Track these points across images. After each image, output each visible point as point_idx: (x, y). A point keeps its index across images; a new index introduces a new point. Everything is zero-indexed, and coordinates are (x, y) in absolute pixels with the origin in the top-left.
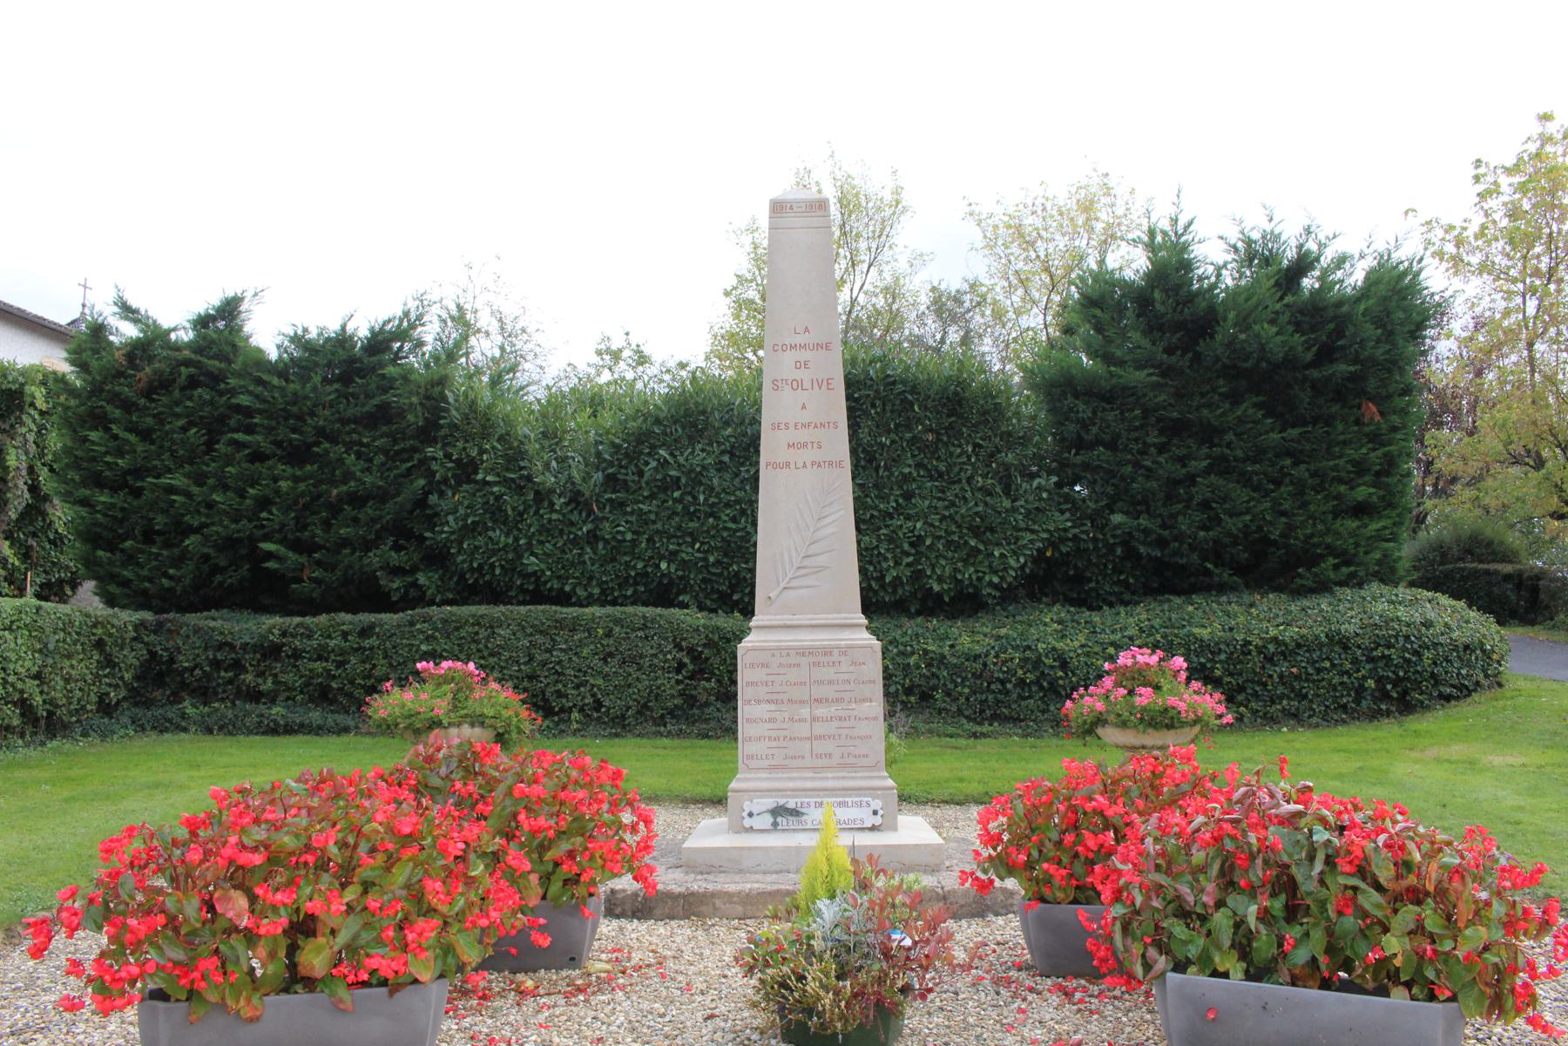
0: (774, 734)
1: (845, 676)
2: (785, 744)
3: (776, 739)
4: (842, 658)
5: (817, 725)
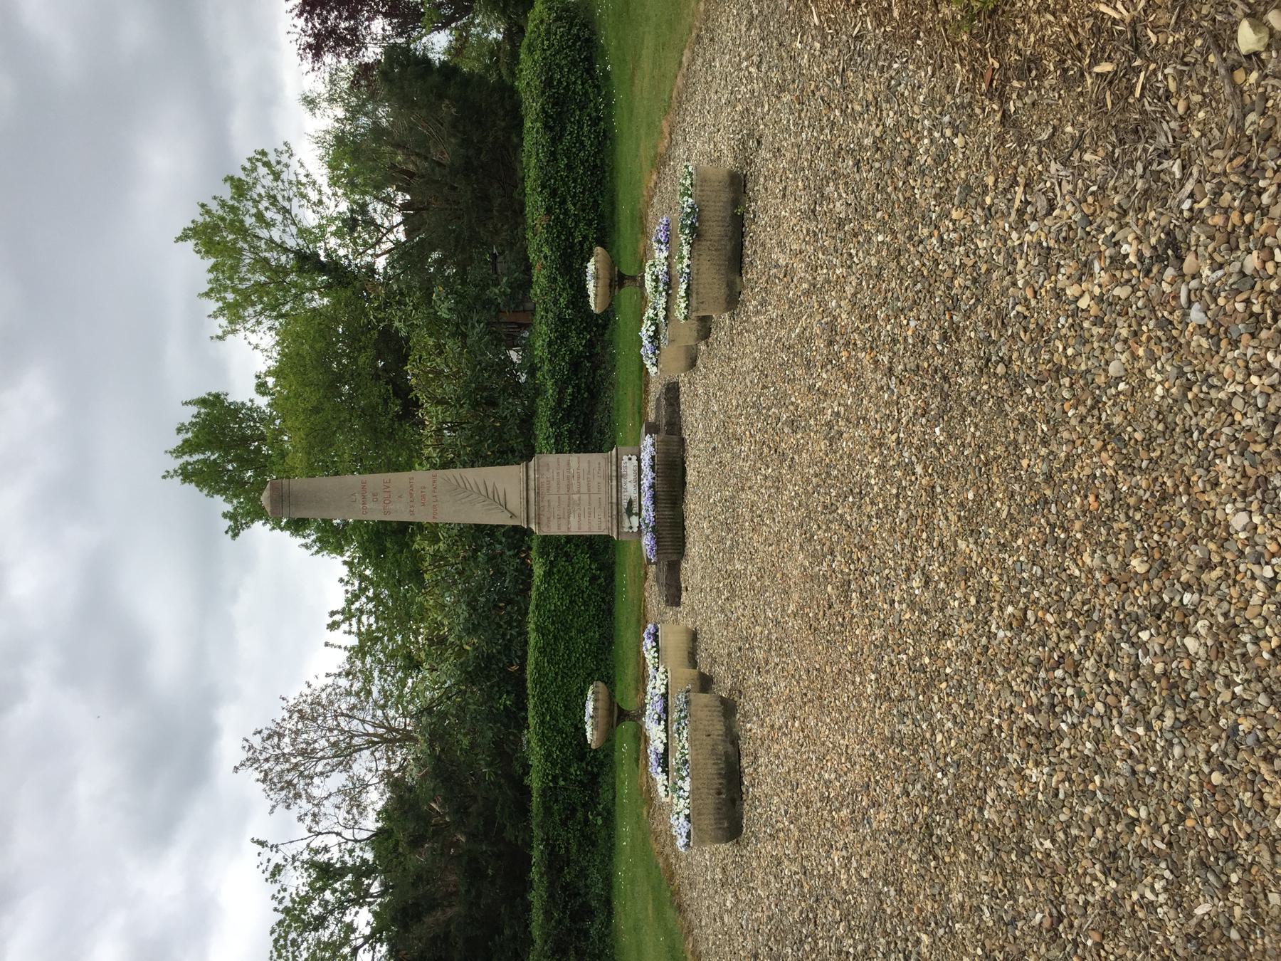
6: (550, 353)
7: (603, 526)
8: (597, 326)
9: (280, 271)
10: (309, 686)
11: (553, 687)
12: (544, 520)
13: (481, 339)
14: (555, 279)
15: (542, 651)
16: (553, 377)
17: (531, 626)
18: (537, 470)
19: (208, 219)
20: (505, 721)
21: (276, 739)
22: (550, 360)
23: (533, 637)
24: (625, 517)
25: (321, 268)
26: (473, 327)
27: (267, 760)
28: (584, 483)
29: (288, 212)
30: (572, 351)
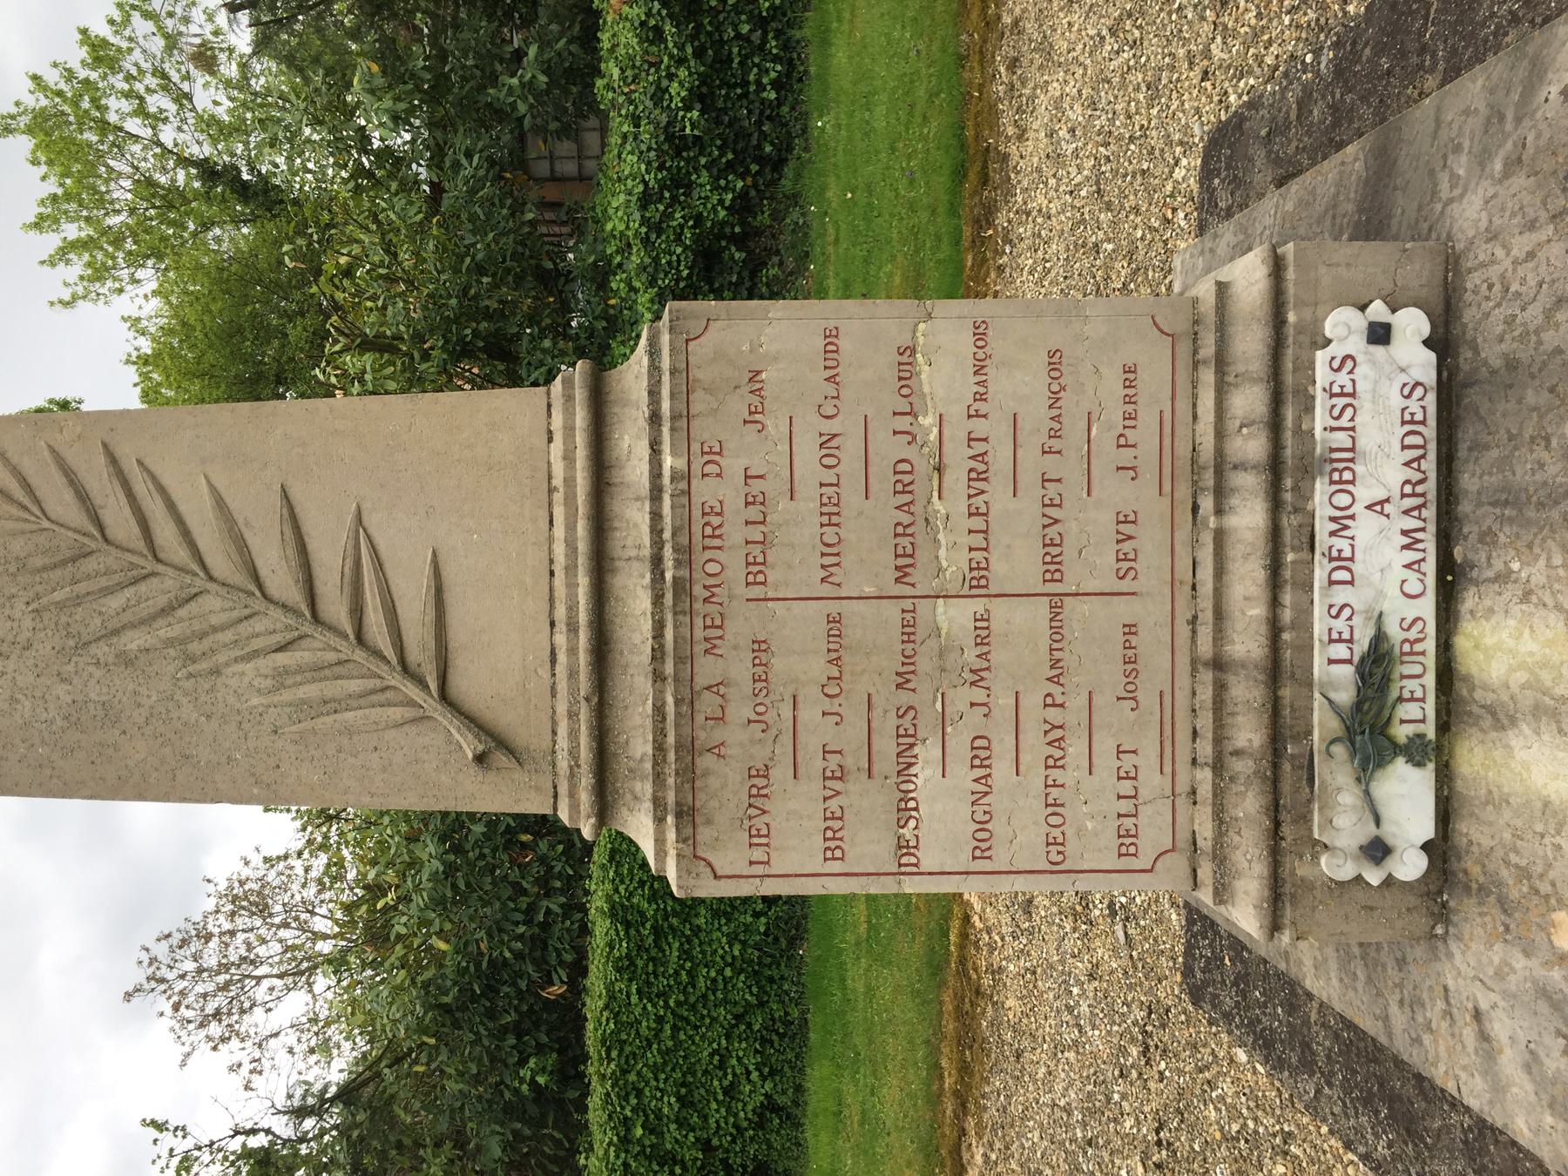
0: (1035, 747)
1: (807, 451)
2: (1077, 702)
3: (1055, 736)
4: (734, 465)
5: (1002, 572)
6: (644, 221)
7: (1154, 831)
8: (761, 160)
9: (172, 200)
10: (247, 863)
11: (653, 1056)
12: (724, 783)
13: (473, 192)
14: (658, 30)
15: (625, 967)
16: (652, 283)
17: (597, 903)
18: (674, 418)
19: (44, 102)
20: (533, 1110)
21: (195, 945)
22: (646, 241)
23: (601, 929)
24: (1336, 773)
25: (243, 191)
26: (457, 166)
27: (182, 977)
28: (1014, 516)
29: (189, 97)
30: (699, 220)
